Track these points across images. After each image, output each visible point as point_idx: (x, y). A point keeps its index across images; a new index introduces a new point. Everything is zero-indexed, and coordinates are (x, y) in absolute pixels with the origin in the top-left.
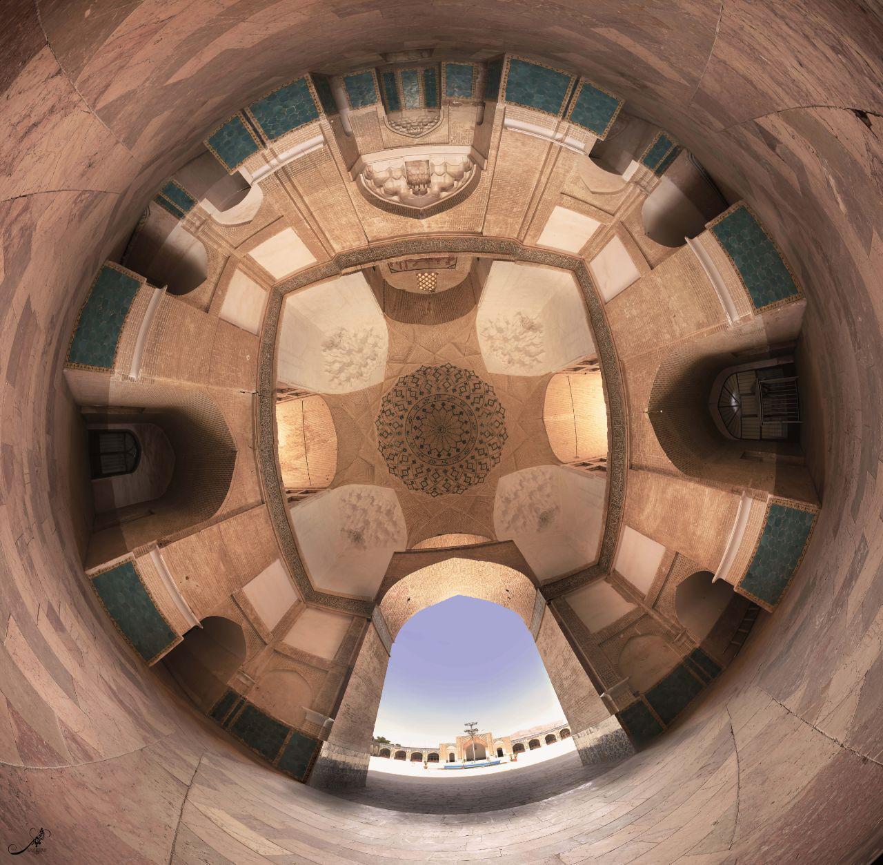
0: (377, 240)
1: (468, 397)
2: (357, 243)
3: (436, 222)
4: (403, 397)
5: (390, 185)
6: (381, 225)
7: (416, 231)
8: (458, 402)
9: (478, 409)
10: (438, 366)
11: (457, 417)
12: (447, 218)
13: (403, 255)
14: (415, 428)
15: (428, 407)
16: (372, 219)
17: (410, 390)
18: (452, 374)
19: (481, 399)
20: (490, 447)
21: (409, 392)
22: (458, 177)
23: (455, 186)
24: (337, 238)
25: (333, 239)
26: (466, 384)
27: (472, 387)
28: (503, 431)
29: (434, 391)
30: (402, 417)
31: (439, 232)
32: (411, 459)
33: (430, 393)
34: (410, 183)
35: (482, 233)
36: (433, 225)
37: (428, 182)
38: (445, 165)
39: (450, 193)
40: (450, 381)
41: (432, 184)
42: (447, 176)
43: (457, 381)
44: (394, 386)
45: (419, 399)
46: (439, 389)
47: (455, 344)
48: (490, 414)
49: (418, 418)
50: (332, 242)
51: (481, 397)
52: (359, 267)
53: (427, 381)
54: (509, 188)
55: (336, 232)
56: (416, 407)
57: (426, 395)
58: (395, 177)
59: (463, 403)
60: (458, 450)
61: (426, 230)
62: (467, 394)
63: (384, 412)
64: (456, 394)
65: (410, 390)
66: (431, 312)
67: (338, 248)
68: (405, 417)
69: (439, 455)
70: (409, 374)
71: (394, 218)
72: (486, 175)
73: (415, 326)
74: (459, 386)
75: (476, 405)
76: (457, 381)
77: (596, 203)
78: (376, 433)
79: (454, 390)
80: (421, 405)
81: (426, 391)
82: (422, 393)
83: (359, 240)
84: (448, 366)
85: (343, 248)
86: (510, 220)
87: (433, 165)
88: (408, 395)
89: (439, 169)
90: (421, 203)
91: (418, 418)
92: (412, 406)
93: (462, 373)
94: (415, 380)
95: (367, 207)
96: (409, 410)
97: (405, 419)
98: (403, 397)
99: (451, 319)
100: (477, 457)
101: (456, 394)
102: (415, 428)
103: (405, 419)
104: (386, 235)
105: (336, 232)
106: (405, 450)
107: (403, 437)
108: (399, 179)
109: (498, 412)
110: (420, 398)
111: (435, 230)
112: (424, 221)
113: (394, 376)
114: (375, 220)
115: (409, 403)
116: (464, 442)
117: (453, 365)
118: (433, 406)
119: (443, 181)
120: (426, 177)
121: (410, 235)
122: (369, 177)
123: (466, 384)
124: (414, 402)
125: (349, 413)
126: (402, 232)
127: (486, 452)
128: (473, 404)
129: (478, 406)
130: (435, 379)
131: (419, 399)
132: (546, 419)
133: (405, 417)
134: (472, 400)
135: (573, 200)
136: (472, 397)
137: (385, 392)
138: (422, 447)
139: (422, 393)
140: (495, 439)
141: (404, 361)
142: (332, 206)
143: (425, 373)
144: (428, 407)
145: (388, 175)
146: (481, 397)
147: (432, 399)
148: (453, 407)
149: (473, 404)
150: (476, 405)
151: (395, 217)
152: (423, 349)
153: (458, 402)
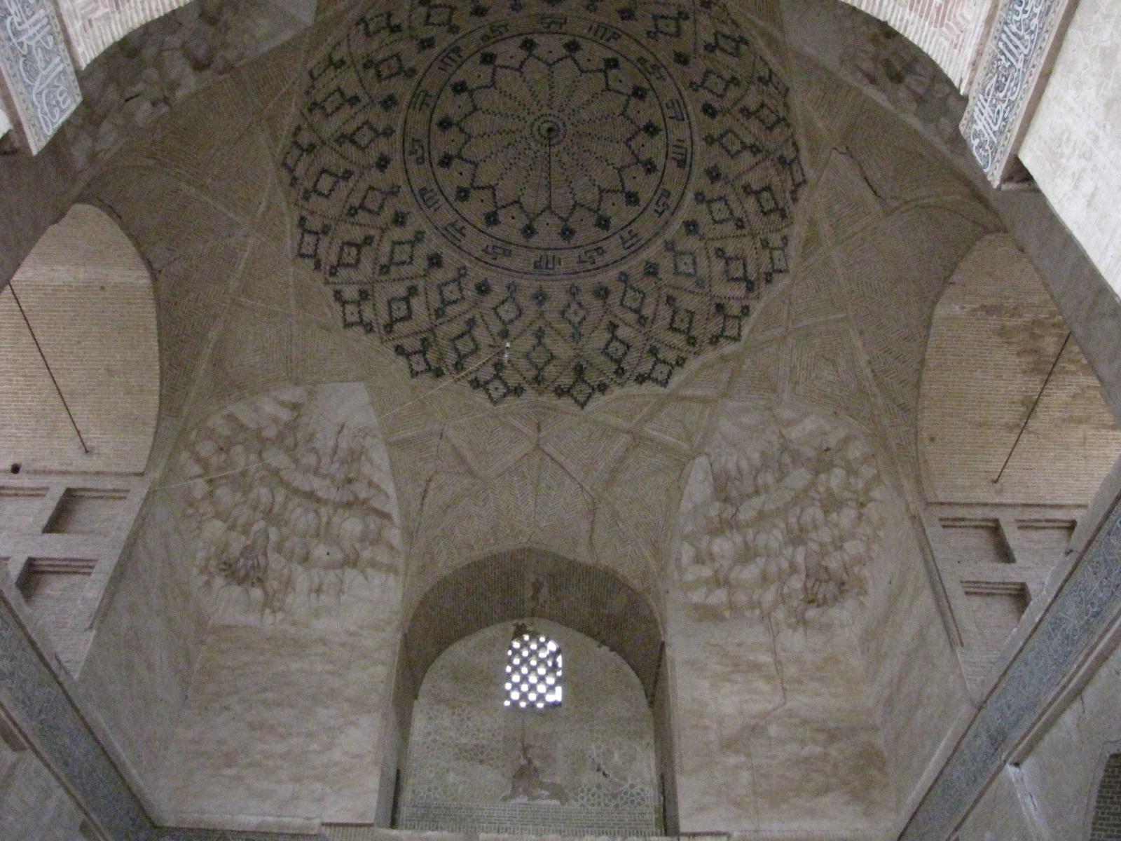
1: (435, 261)
4: (670, 300)
8: (474, 242)
9: (399, 220)
10: (530, 395)
11: (483, 179)
14: (650, 167)
15: (586, 232)
17: (642, 320)
18: (485, 355)
19: (384, 260)
20: (349, 93)
21: (648, 311)
26: (439, 313)
27: (417, 303)
28: (300, 170)
29: (557, 293)
30: (691, 227)
32: (696, 70)
33: (574, 292)
40: (496, 327)
43: (471, 323)
44: (693, 364)
45: (613, 273)
46: (540, 297)
47: (470, 472)
48: (353, 211)
49: (632, 199)
51: (385, 269)
53: (576, 336)
56: (633, 245)
57: (587, 283)
59: (453, 234)
60: (488, 59)
62: (438, 275)
63: (750, 286)
64: (477, 273)
65: (642, 320)
66: (532, 578)
68: (676, 225)
69: (573, 47)
70: (633, 388)
73: (583, 555)
74: (464, 306)
75: (406, 233)
76: (471, 323)
78: (798, 231)
79: (483, 289)
80: (614, 248)
81: (586, 298)
82: (602, 293)
84: (497, 389)
88: (650, 300)
91: (632, 199)
92: (645, 255)
93: (452, 358)
94: (617, 349)
96: (660, 242)
97: (683, 215)
98: (670, 300)
99: (476, 567)
100: (407, 48)
101: (477, 273)
102: (650, 167)
103: (683, 215)
106: (709, 111)
107: (703, 157)
109: (325, 230)
110: (608, 277)
113: (682, 399)
115: (651, 270)
116: (460, 88)
117: (480, 397)
118: (567, 233)
123: (439, 313)
124: (634, 266)
125: (863, 359)
127: (372, 72)
128: (419, 237)
129: (396, 233)
130: (547, 341)
131: (613, 273)
132: (140, 278)
133: (676, 225)
134: (423, 251)
136: (421, 264)
137: (724, 359)
138: (639, 93)
139: (602, 293)
140: (330, 128)
141: (638, 440)
143: (579, 371)
144: (586, 232)
146: (385, 269)
147: (569, 259)
148: (492, 219)
149: (419, 237)
150: (406, 233)
152: (571, 467)
153: (474, 242)
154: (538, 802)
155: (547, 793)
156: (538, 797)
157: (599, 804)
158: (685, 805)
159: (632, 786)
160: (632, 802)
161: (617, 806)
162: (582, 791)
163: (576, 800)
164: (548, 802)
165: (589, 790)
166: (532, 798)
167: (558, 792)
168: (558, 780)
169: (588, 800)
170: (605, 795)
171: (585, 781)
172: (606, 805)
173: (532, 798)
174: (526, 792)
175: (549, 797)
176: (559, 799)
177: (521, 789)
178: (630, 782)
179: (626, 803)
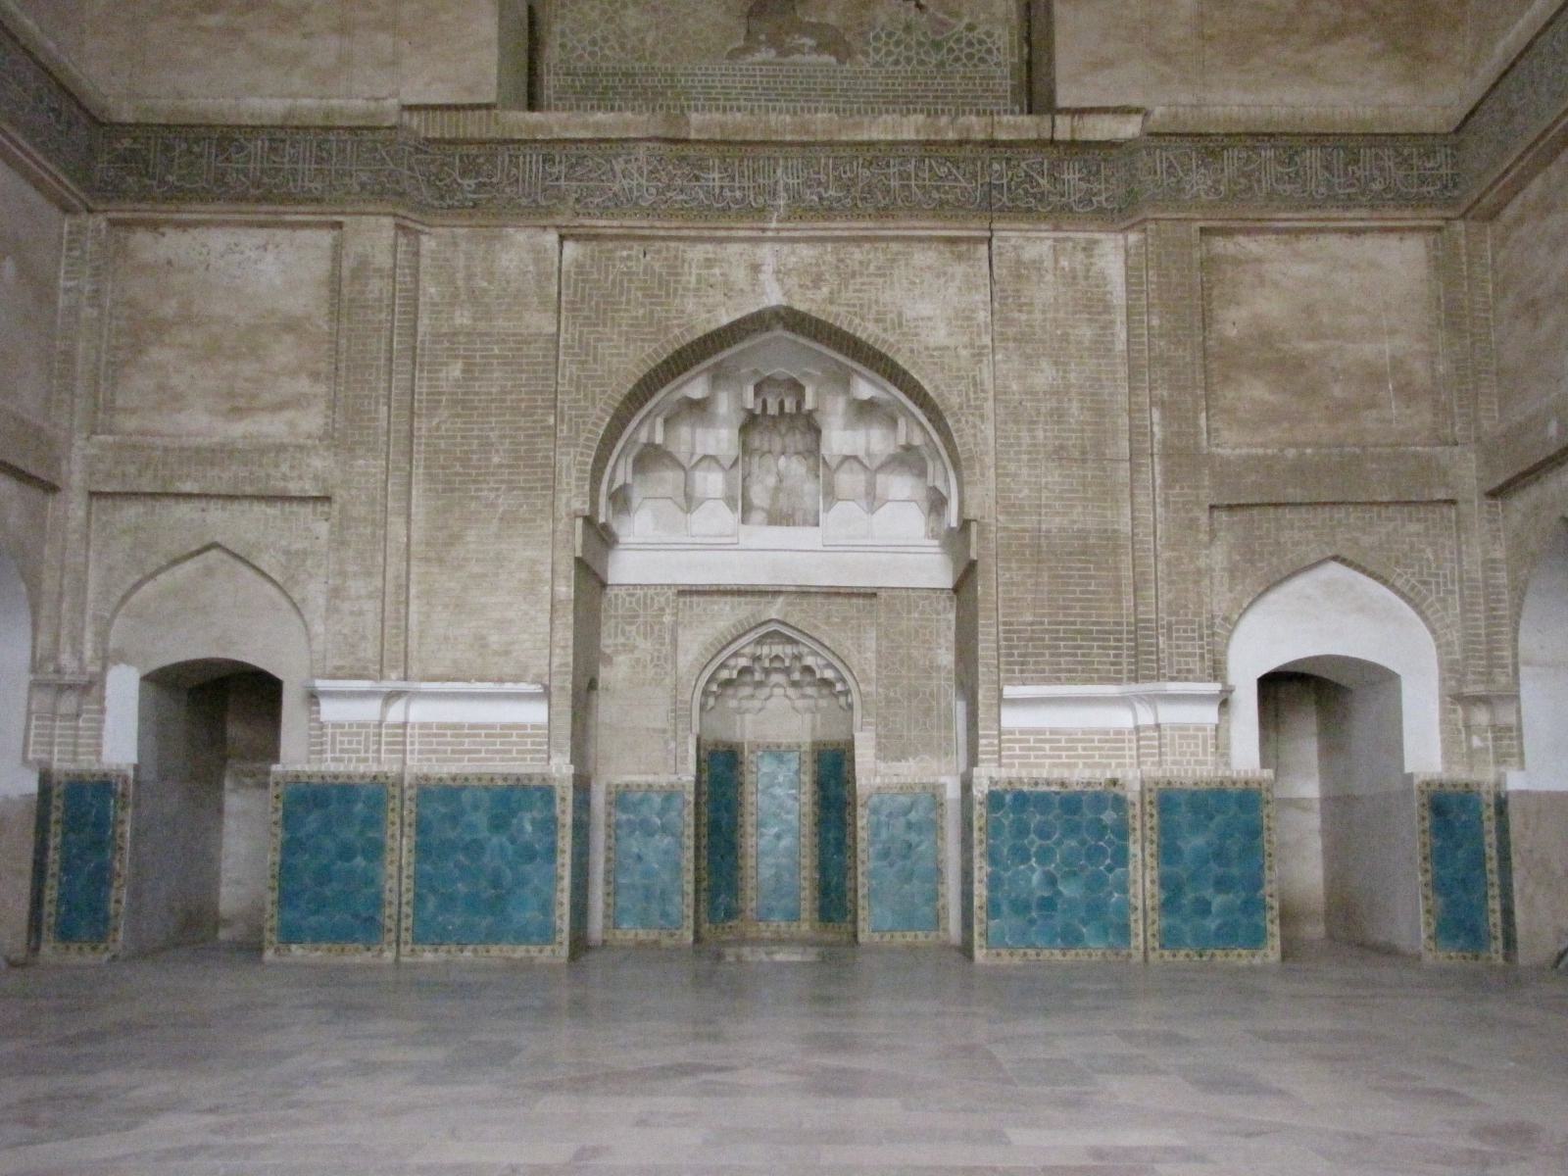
0: (952, 241)
2: (1030, 252)
3: (729, 290)
5: (876, 441)
6: (925, 308)
7: (806, 252)
12: (690, 305)
13: (871, 144)
16: (951, 342)
22: (650, 458)
23: (659, 421)
24: (1095, 305)
25: (1108, 308)
31: (721, 241)
34: (811, 427)
35: (562, 238)
36: (740, 276)
37: (750, 423)
38: (689, 501)
39: (678, 395)
41: (738, 419)
42: (683, 457)
50: (1118, 294)
52: (1064, 128)
54: (496, 460)
55: (1086, 333)
58: (856, 466)
61: (766, 253)
67: (1111, 255)
71: (871, 326)
72: (573, 499)
77: (184, 511)
83: (1019, 262)
85: (1089, 248)
86: (462, 318)
87: (730, 501)
89: (712, 483)
90: (779, 355)
95: (955, 400)
104: (923, 257)
105: (1086, 333)
108: (847, 458)
111: (733, 249)
112: (773, 297)
114: (939, 336)
119: (699, 431)
120: (757, 441)
121: (823, 240)
122: (937, 503)
126: (857, 254)
135: (277, 486)
142: (1059, 454)
145: (881, 478)
151: (867, 331)
154: (797, 57)
155: (810, 42)
156: (799, 49)
157: (909, 60)
158: (1067, 58)
159: (971, 28)
160: (970, 56)
161: (941, 64)
162: (877, 38)
163: (866, 54)
164: (813, 58)
165: (890, 35)
166: (784, 52)
167: (833, 43)
168: (831, 18)
169: (889, 53)
170: (920, 44)
171: (883, 18)
172: (922, 62)
173: (784, 52)
174: (775, 42)
175: (819, 48)
176: (835, 53)
177: (762, 37)
178: (966, 20)
179: (957, 59)
